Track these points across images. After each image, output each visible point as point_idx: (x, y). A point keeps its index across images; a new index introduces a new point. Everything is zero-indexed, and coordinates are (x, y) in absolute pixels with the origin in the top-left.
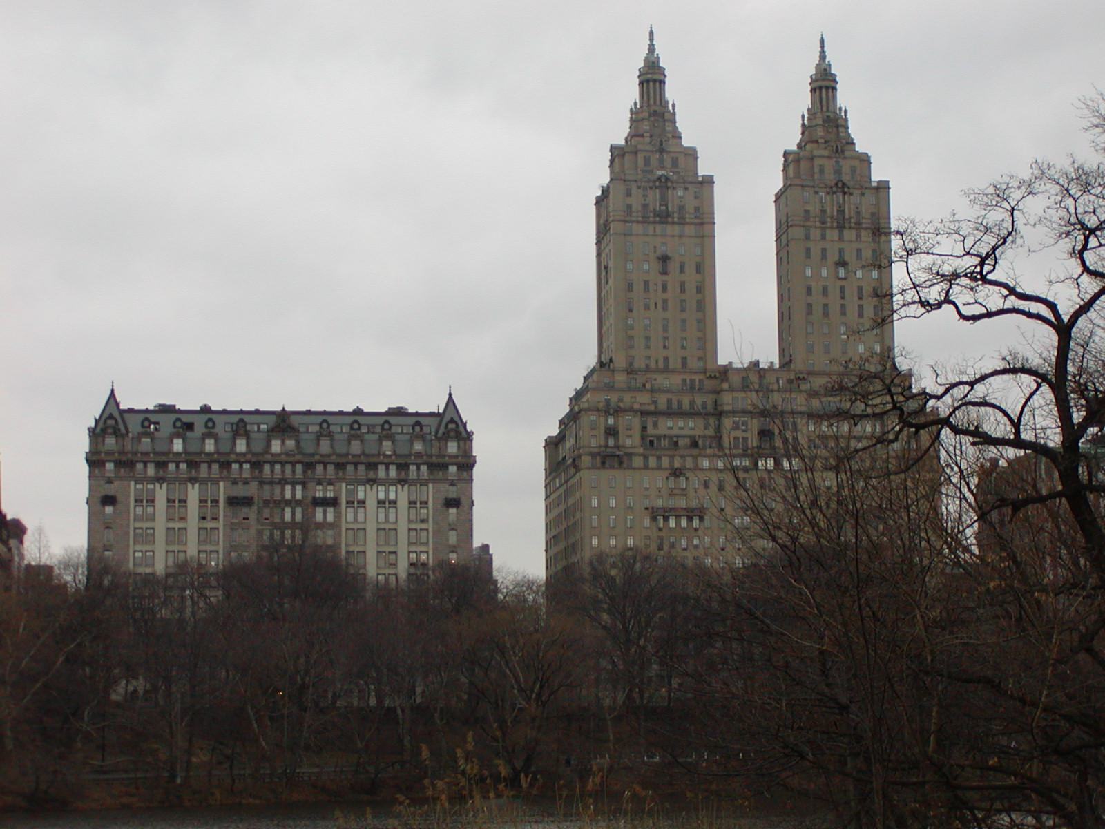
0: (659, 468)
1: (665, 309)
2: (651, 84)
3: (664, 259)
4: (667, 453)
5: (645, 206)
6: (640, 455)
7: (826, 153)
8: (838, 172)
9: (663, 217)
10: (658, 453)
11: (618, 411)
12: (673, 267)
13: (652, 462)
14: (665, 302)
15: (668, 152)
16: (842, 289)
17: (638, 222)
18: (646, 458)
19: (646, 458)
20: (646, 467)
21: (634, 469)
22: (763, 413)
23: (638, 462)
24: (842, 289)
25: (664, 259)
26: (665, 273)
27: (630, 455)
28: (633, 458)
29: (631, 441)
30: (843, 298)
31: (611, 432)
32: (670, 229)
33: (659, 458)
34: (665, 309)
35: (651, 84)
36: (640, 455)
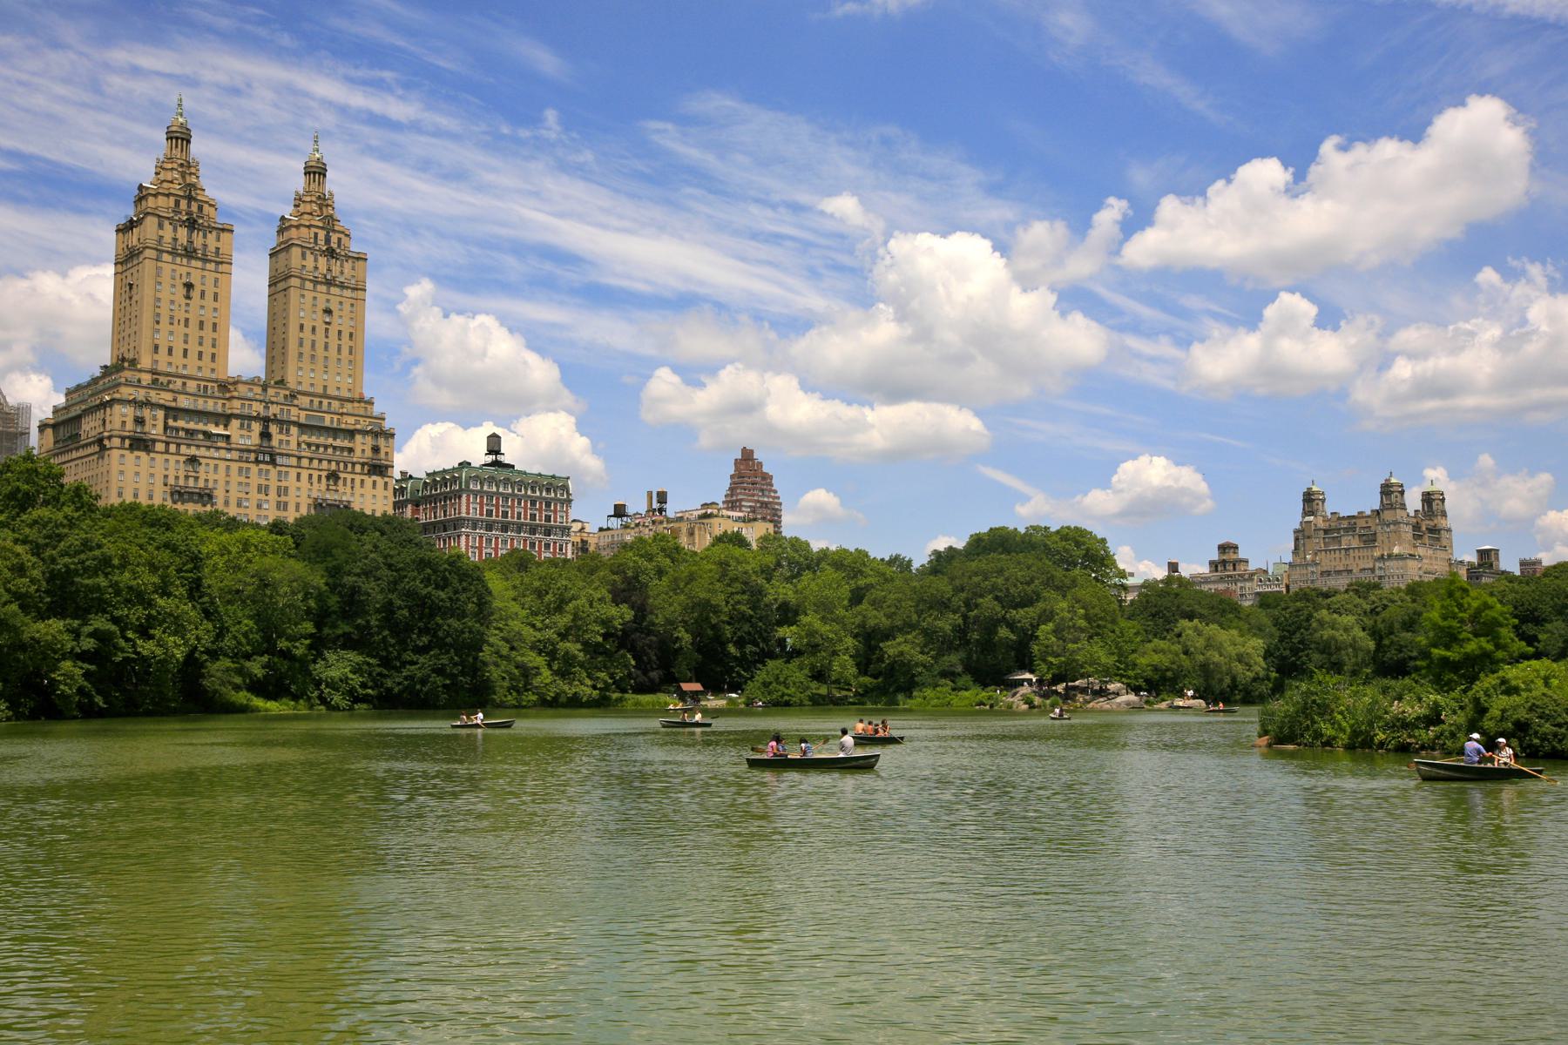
0: (178, 453)
1: (186, 325)
2: (180, 141)
3: (189, 286)
4: (185, 441)
5: (175, 240)
6: (162, 442)
7: (321, 224)
8: (328, 240)
9: (190, 253)
10: (178, 441)
11: (147, 403)
12: (195, 294)
13: (173, 448)
14: (187, 320)
15: (196, 200)
16: (327, 330)
17: (168, 252)
18: (167, 444)
19: (167, 444)
20: (167, 452)
21: (157, 452)
22: (266, 421)
23: (160, 447)
24: (327, 330)
25: (189, 286)
26: (188, 297)
27: (154, 441)
28: (157, 444)
29: (155, 430)
30: (327, 337)
31: (139, 421)
32: (194, 263)
33: (178, 445)
34: (186, 325)
35: (180, 141)
36: (162, 442)
